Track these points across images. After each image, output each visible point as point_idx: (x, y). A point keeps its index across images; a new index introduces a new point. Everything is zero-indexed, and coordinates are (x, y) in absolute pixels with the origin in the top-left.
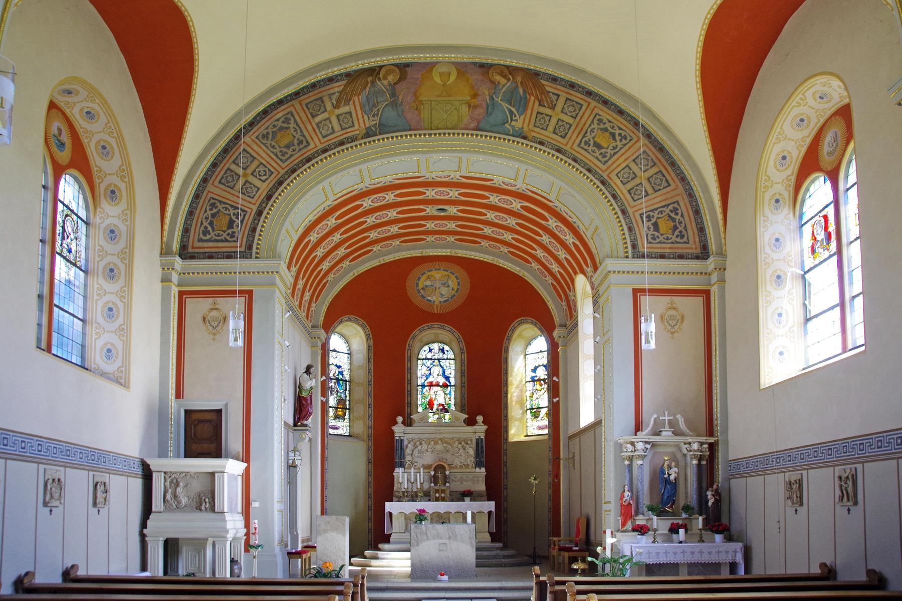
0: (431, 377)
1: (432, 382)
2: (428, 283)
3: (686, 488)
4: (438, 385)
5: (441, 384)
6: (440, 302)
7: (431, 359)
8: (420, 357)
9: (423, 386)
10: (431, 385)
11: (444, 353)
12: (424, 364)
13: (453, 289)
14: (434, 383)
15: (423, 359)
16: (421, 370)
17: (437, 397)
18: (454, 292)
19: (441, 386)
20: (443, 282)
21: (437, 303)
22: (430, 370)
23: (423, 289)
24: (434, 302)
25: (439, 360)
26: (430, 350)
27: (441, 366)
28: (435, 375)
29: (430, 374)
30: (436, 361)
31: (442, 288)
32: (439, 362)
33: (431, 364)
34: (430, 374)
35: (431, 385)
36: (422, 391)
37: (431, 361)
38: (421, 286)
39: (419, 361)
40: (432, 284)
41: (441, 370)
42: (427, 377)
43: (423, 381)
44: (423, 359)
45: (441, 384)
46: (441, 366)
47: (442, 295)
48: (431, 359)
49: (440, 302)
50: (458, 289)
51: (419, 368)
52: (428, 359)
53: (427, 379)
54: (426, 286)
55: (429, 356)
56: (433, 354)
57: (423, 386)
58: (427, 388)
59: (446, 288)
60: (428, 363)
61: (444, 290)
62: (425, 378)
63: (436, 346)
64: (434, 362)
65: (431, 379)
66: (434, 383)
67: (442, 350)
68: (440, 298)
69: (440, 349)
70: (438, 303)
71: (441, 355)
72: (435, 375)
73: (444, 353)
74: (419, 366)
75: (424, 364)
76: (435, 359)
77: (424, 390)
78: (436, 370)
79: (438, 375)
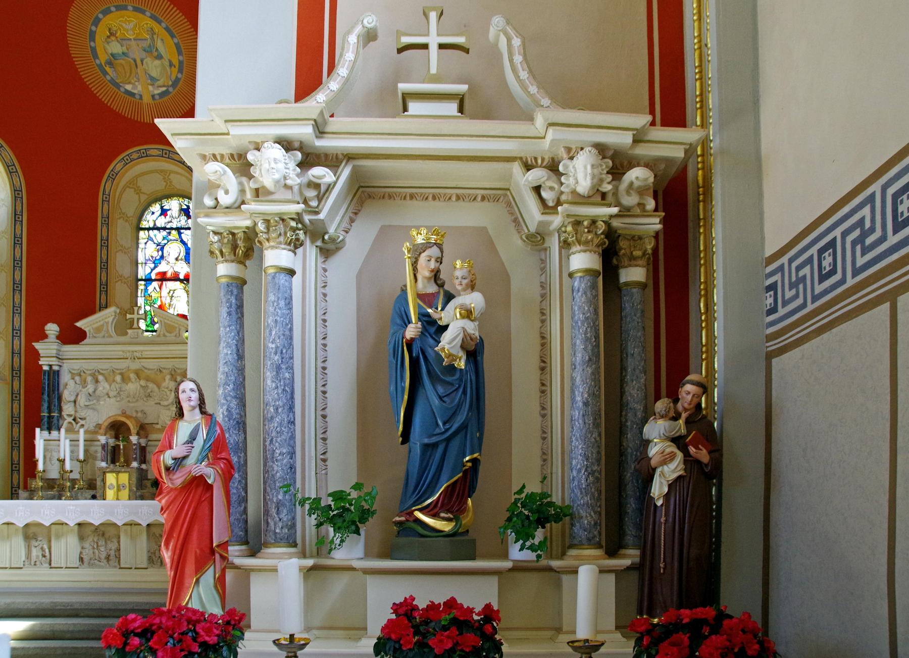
0: (163, 262)
1: (164, 273)
2: (115, 48)
3: (545, 411)
4: (176, 278)
5: (182, 277)
6: (153, 96)
7: (164, 229)
8: (144, 224)
9: (148, 280)
10: (163, 278)
11: (189, 217)
12: (150, 239)
13: (171, 65)
14: (169, 275)
15: (149, 229)
16: (147, 250)
17: (174, 302)
18: (175, 70)
19: (181, 281)
20: (145, 44)
21: (147, 99)
22: (162, 249)
23: (110, 63)
24: (141, 96)
25: (178, 229)
26: (164, 212)
27: (183, 242)
28: (172, 259)
29: (162, 257)
30: (174, 232)
31: (148, 60)
32: (180, 234)
33: (164, 238)
34: (162, 257)
35: (163, 278)
36: (146, 290)
37: (164, 233)
38: (103, 58)
39: (142, 234)
40: (124, 49)
41: (183, 249)
42: (156, 263)
43: (148, 270)
44: (149, 229)
45: (182, 277)
46: (183, 242)
47: (153, 79)
48: (164, 229)
49: (153, 96)
50: (181, 63)
51: (141, 246)
52: (159, 229)
53: (155, 267)
54: (112, 55)
55: (161, 222)
56: (168, 219)
57: (148, 280)
58: (155, 284)
59: (157, 62)
60: (159, 236)
61: (154, 67)
62: (152, 266)
63: (173, 205)
64: (169, 233)
65: (163, 267)
66: (169, 275)
67: (186, 212)
68: (151, 88)
69: (181, 210)
70: (151, 101)
71: (183, 221)
72: (172, 259)
73: (189, 217)
74: (142, 242)
75: (150, 239)
76: (172, 229)
77: (150, 288)
78: (174, 249)
79: (177, 259)
